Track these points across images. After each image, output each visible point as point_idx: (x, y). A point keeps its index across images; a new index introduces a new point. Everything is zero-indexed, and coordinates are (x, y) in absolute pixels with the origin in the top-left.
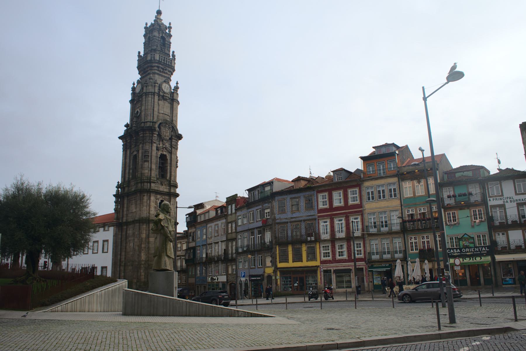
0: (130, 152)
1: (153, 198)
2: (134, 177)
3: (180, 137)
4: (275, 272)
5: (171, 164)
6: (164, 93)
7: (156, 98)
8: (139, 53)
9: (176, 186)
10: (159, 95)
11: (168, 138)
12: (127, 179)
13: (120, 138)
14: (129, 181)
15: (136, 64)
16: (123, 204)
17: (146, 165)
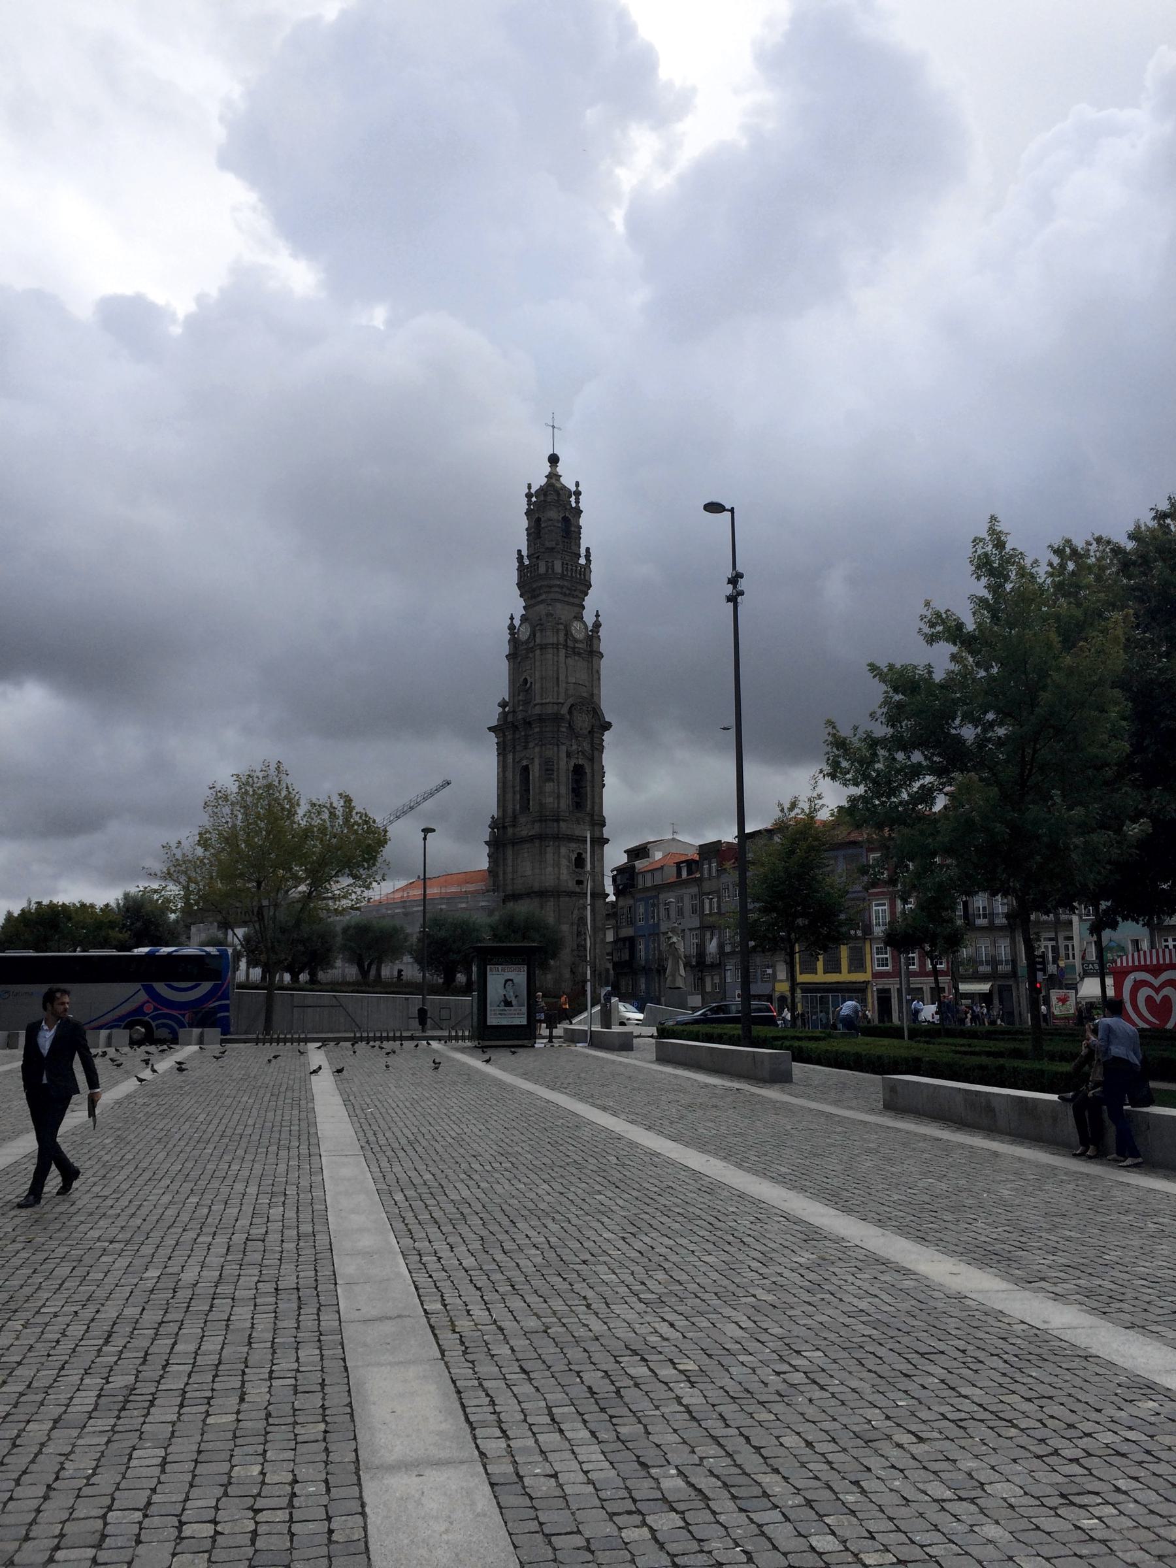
0: (514, 759)
1: (563, 850)
2: (525, 808)
3: (607, 726)
4: (793, 990)
5: (592, 782)
6: (576, 640)
7: (562, 652)
8: (519, 552)
9: (603, 824)
10: (566, 646)
11: (586, 732)
12: (510, 811)
13: (490, 729)
14: (515, 817)
15: (514, 577)
16: (505, 859)
17: (549, 787)
